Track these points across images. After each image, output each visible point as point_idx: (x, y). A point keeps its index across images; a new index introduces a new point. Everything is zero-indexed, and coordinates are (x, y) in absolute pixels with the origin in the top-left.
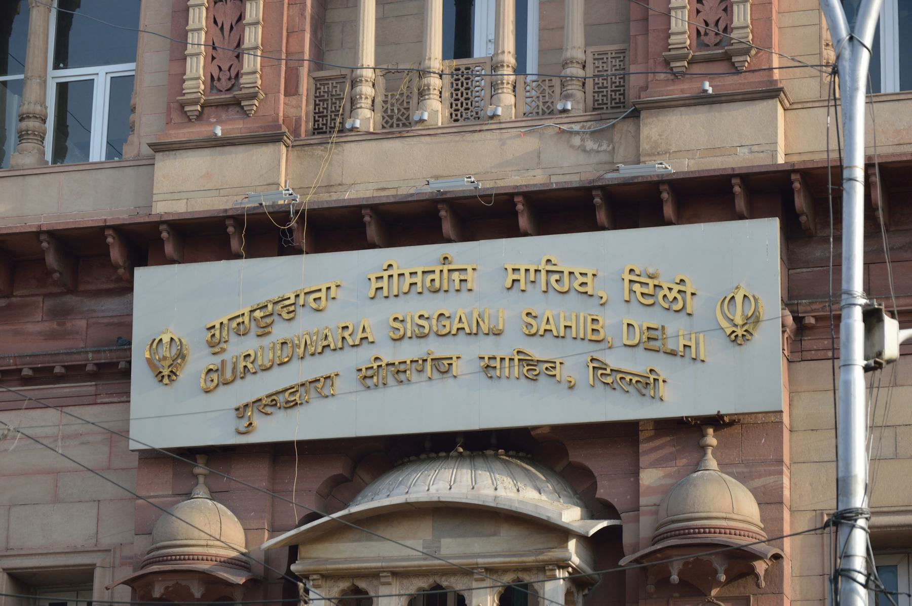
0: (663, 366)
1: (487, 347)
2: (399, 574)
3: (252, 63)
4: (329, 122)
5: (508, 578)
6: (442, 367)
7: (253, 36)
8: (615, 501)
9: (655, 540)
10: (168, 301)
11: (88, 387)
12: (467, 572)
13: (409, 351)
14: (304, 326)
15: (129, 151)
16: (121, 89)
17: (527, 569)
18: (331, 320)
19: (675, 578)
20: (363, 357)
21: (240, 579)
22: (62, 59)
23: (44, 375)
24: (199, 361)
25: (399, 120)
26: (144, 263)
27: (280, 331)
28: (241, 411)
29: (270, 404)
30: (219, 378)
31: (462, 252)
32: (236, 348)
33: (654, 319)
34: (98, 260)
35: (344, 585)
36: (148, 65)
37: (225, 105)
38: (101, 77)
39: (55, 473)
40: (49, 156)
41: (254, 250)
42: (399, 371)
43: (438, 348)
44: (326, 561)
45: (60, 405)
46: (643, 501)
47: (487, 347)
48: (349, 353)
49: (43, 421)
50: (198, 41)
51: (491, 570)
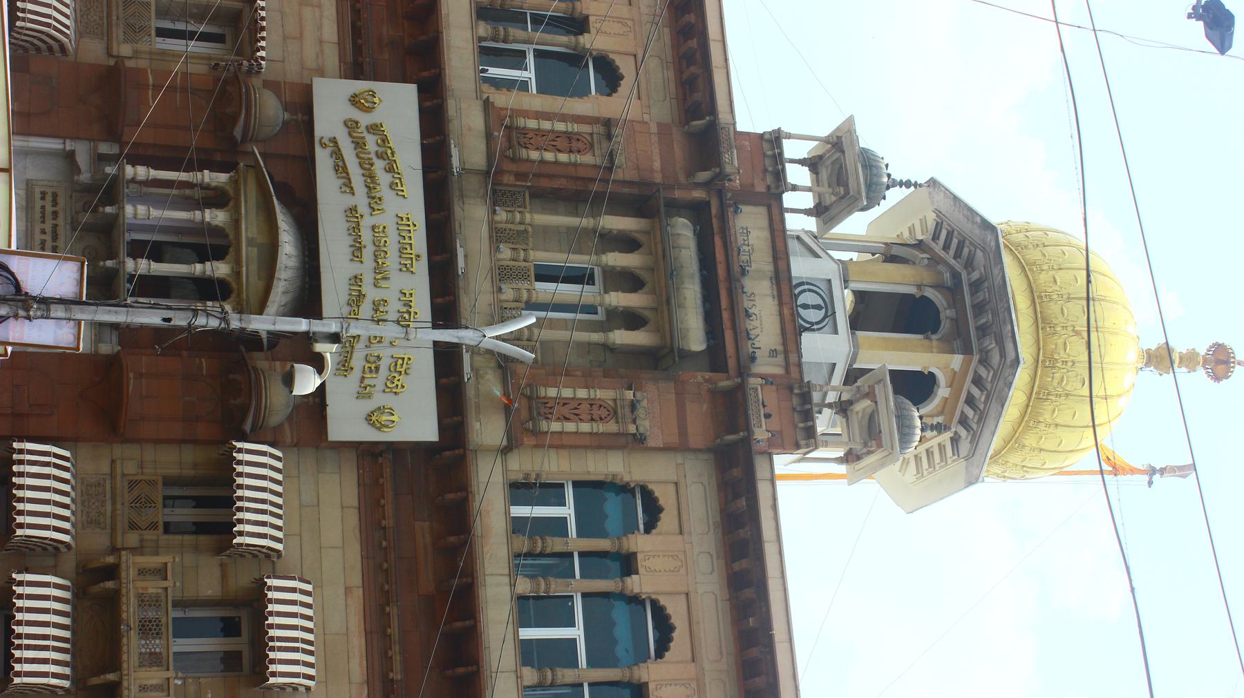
0: (356, 375)
1: (368, 278)
2: (236, 223)
3: (534, 155)
4: (498, 197)
5: (234, 285)
6: (357, 250)
7: (549, 156)
8: (278, 348)
9: (255, 369)
10: (398, 104)
11: (350, 58)
12: (238, 262)
13: (366, 236)
14: (384, 178)
15: (485, 87)
16: (524, 86)
17: (239, 295)
18: (383, 190)
19: (231, 376)
20: (363, 209)
21: (238, 132)
22: (539, 54)
23: (356, 32)
24: (365, 119)
25: (498, 235)
26: (420, 91)
27: (379, 165)
28: (334, 141)
29: (337, 154)
30: (351, 125)
31: (422, 268)
32: (371, 142)
33: (384, 371)
34: (421, 62)
35: (231, 193)
36: (534, 100)
37: (509, 140)
38: (529, 74)
39: (300, 37)
40: (484, 44)
41: (425, 150)
42: (355, 229)
43: (368, 253)
44: (245, 184)
45: (341, 43)
46: (278, 363)
47: (368, 278)
48: (367, 201)
49: (330, 31)
50: (546, 125)
51: (237, 274)
